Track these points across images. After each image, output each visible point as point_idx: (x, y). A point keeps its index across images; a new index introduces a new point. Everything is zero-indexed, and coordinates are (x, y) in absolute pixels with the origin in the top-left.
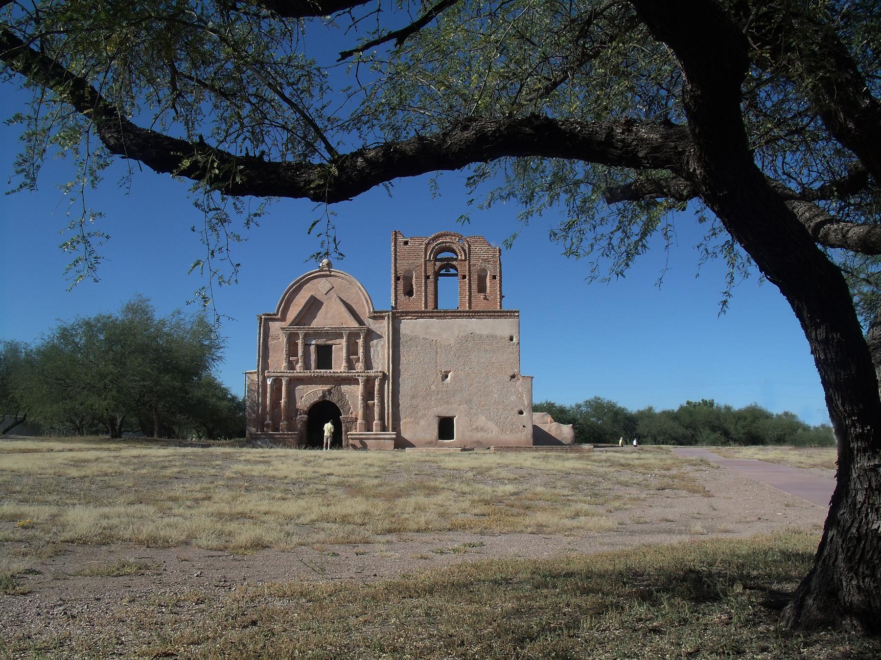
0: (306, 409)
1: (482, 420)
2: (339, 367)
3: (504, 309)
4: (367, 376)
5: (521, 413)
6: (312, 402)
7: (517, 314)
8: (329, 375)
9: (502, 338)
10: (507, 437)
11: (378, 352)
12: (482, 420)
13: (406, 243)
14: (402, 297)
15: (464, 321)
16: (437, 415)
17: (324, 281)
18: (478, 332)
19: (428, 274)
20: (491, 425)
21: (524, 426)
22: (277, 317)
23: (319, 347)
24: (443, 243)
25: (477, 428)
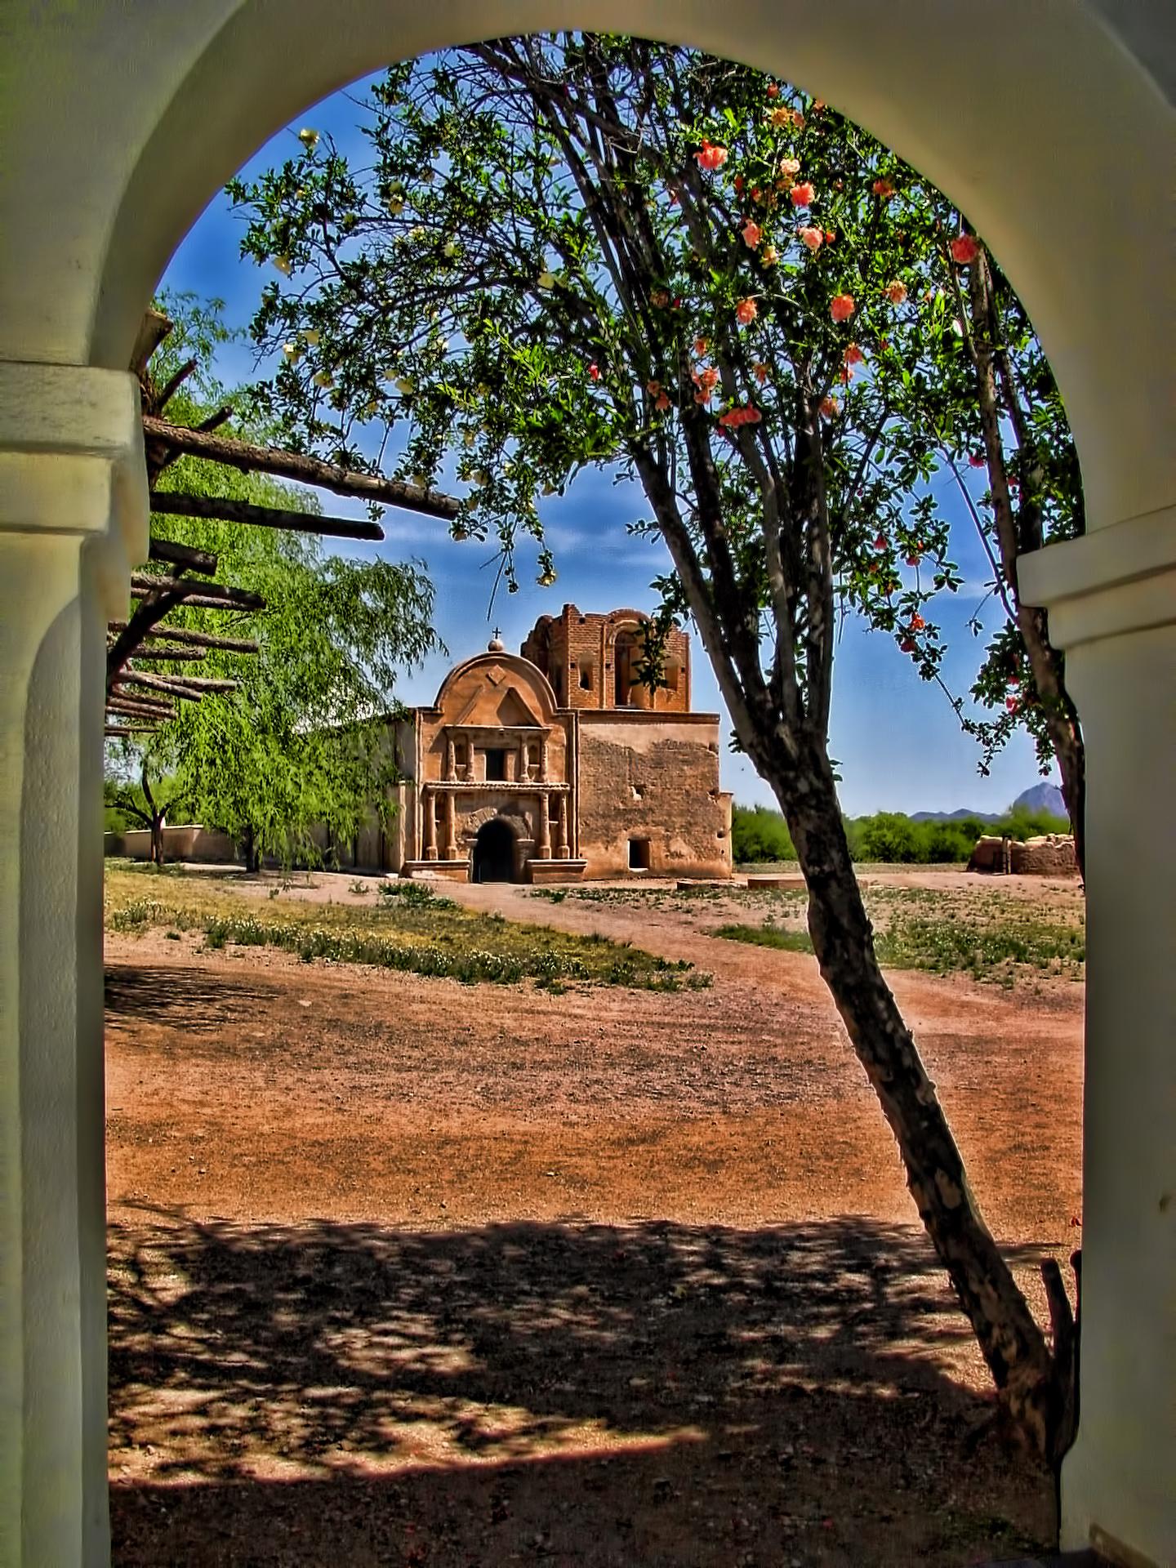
1: (679, 845)
3: (691, 711)
5: (720, 835)
12: (679, 845)
13: (582, 621)
20: (685, 850)
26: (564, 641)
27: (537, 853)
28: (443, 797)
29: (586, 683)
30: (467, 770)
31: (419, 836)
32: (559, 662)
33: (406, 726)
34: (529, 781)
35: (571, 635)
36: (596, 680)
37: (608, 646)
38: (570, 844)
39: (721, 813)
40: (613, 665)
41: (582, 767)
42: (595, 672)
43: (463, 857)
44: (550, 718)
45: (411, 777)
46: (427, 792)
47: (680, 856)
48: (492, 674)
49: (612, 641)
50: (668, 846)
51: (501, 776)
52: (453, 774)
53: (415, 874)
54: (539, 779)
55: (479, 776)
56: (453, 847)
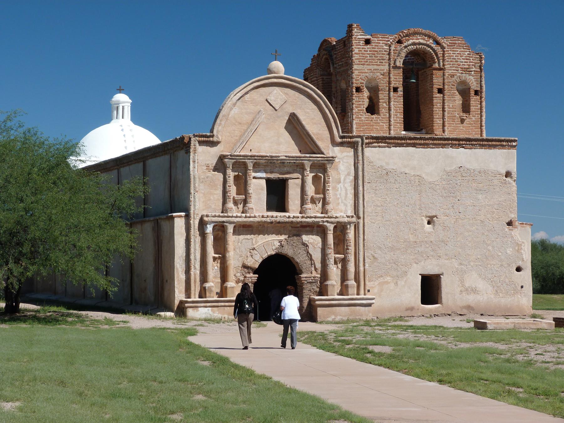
0: (257, 266)
3: (485, 136)
4: (338, 222)
5: (519, 269)
6: (265, 256)
7: (514, 144)
8: (287, 220)
9: (496, 174)
10: (503, 300)
11: (346, 190)
14: (366, 116)
15: (450, 151)
16: (420, 273)
17: (275, 92)
18: (468, 166)
19: (395, 86)
20: (481, 285)
21: (522, 287)
22: (215, 139)
24: (414, 44)
25: (467, 290)
26: (348, 64)
27: (323, 291)
28: (220, 229)
29: (372, 109)
30: (245, 202)
32: (343, 85)
33: (182, 153)
35: (355, 57)
36: (383, 105)
37: (395, 67)
38: (357, 279)
39: (518, 246)
40: (401, 89)
42: (383, 96)
44: (334, 143)
45: (187, 210)
46: (202, 224)
47: (475, 291)
48: (271, 99)
49: (400, 63)
50: (462, 281)
52: (230, 205)
53: (191, 313)
54: (324, 211)
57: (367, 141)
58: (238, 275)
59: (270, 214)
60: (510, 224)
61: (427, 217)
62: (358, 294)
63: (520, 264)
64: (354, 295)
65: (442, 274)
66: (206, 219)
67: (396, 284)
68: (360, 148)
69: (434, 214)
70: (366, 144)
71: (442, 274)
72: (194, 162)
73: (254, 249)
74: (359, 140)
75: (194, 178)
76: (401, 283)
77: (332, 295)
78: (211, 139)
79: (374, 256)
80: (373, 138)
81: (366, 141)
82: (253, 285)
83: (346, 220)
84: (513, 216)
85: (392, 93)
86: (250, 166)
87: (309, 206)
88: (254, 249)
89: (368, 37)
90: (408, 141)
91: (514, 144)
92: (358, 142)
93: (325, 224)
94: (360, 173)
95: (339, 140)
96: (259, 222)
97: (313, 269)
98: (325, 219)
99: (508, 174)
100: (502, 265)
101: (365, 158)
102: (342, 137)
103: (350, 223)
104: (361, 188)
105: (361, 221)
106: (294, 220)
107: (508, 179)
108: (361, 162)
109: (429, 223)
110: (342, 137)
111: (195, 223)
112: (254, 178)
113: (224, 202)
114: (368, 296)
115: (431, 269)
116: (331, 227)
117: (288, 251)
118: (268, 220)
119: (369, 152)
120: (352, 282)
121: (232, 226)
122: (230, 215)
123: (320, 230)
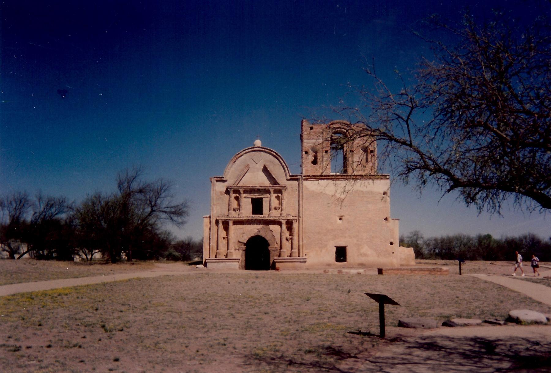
0: (245, 242)
1: (365, 249)
2: (266, 214)
5: (391, 243)
6: (250, 236)
7: (388, 177)
20: (369, 252)
21: (393, 253)
22: (224, 179)
23: (253, 200)
25: (361, 255)
29: (315, 162)
31: (213, 244)
34: (275, 215)
36: (319, 160)
41: (305, 205)
42: (319, 155)
43: (238, 255)
46: (217, 222)
47: (365, 255)
51: (262, 214)
52: (231, 211)
55: (247, 211)
56: (232, 250)
57: (305, 178)
58: (236, 246)
59: (254, 216)
60: (386, 219)
61: (338, 216)
62: (299, 256)
63: (392, 240)
64: (295, 257)
65: (347, 246)
66: (218, 218)
67: (321, 251)
68: (301, 182)
69: (342, 215)
70: (304, 179)
71: (347, 246)
72: (213, 190)
73: (244, 233)
74: (300, 177)
75: (213, 199)
76: (324, 251)
77: (283, 257)
78: (222, 179)
79: (308, 237)
80: (308, 176)
81: (304, 178)
82: (244, 253)
83: (292, 218)
84: (388, 215)
85: (324, 154)
86: (242, 192)
87: (273, 211)
88: (244, 233)
89: (311, 126)
90: (328, 177)
91: (388, 177)
92: (299, 179)
93: (281, 220)
94: (301, 194)
95: (289, 178)
96: (245, 220)
97: (276, 243)
98: (280, 218)
99: (385, 193)
100: (381, 241)
101: (304, 186)
102: (290, 176)
103: (294, 220)
104: (301, 202)
105: (301, 219)
106: (264, 218)
107: (385, 196)
108: (301, 188)
109: (340, 219)
110: (290, 176)
111: (214, 221)
112: (245, 198)
113: (229, 210)
114: (305, 257)
115: (341, 244)
116: (284, 222)
117: (262, 234)
118: (250, 218)
119: (306, 183)
120: (295, 250)
121: (232, 221)
122: (230, 216)
123: (280, 223)
